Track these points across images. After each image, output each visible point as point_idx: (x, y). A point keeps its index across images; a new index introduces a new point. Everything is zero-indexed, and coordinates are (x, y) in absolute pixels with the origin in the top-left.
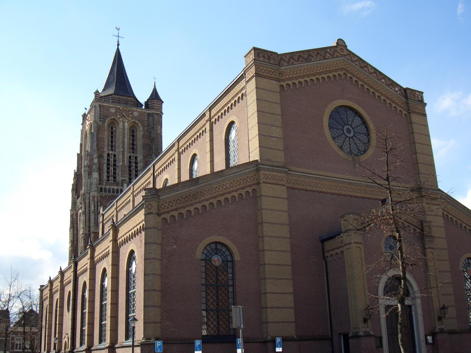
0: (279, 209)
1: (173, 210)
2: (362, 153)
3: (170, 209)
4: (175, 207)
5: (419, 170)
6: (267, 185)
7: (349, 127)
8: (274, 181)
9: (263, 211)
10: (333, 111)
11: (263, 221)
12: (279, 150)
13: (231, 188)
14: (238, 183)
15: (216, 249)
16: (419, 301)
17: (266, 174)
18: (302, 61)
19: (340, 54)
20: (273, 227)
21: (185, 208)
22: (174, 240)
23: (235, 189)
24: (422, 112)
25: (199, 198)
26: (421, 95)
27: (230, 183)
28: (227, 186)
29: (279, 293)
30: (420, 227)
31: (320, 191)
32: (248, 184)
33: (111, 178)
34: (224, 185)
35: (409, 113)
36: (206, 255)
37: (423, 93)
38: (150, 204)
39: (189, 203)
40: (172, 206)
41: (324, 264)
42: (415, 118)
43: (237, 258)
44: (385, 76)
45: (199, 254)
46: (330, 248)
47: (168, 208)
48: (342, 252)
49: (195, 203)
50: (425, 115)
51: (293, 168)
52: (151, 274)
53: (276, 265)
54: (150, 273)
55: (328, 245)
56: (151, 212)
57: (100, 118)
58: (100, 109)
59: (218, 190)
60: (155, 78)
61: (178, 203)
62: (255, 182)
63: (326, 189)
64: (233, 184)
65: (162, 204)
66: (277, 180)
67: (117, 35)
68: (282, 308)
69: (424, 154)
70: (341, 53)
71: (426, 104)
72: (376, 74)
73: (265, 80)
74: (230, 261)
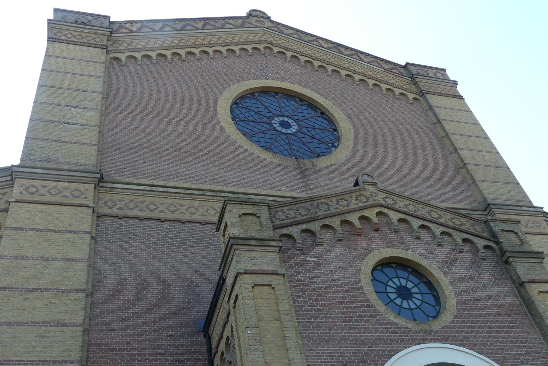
0: (59, 256)
5: (472, 177)
12: (84, 144)
26: (442, 72)
30: (485, 234)
31: (204, 221)
37: (445, 70)
44: (357, 52)
71: (455, 83)
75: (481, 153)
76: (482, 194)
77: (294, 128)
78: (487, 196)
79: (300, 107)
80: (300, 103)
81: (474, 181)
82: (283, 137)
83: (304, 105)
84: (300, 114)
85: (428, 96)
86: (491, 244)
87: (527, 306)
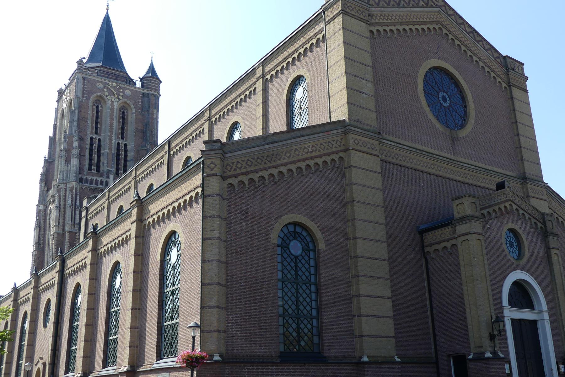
1: (242, 174)
2: (459, 127)
3: (238, 171)
4: (245, 170)
5: (522, 156)
6: (358, 153)
7: (445, 94)
8: (365, 149)
9: (354, 186)
10: (427, 72)
11: (354, 199)
12: (370, 110)
13: (314, 152)
14: (322, 147)
15: (295, 232)
16: (546, 316)
17: (356, 139)
18: (393, 5)
19: (435, 4)
20: (365, 209)
21: (257, 172)
22: (243, 215)
23: (318, 154)
24: (523, 87)
25: (275, 161)
27: (313, 146)
28: (309, 150)
29: (375, 297)
30: (541, 221)
32: (334, 149)
34: (305, 147)
35: (510, 86)
36: (283, 239)
38: (212, 163)
39: (262, 166)
40: (240, 168)
41: (424, 263)
42: (516, 93)
43: (322, 246)
45: (275, 237)
46: (434, 240)
47: (235, 170)
48: (454, 245)
49: (270, 167)
50: (526, 91)
51: (386, 136)
52: (214, 260)
53: (371, 258)
54: (212, 259)
55: (430, 237)
56: (214, 173)
57: (83, 93)
58: (84, 83)
59: (298, 154)
61: (248, 165)
62: (342, 148)
63: (422, 166)
64: (315, 147)
65: (228, 165)
66: (369, 148)
68: (378, 317)
69: (527, 137)
70: (436, 3)
71: (527, 78)
72: (474, 35)
73: (353, 20)
74: (312, 250)
75: (529, 140)
76: (524, 169)
77: (447, 104)
78: (527, 171)
79: (457, 95)
80: (459, 93)
81: (522, 160)
82: (439, 105)
83: (460, 95)
84: (455, 99)
85: (513, 88)
86: (543, 227)
87: (548, 259)
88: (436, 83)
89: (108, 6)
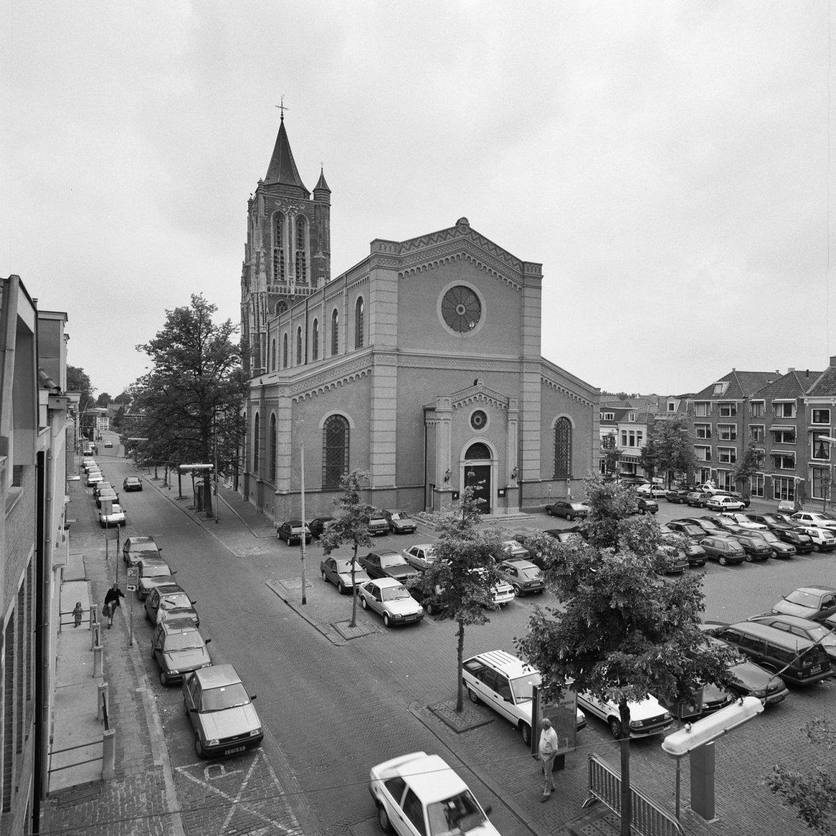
33: (279, 276)
55: (429, 415)
57: (265, 212)
58: (265, 201)
60: (322, 163)
62: (371, 364)
67: (280, 105)
88: (455, 298)
89: (282, 115)
